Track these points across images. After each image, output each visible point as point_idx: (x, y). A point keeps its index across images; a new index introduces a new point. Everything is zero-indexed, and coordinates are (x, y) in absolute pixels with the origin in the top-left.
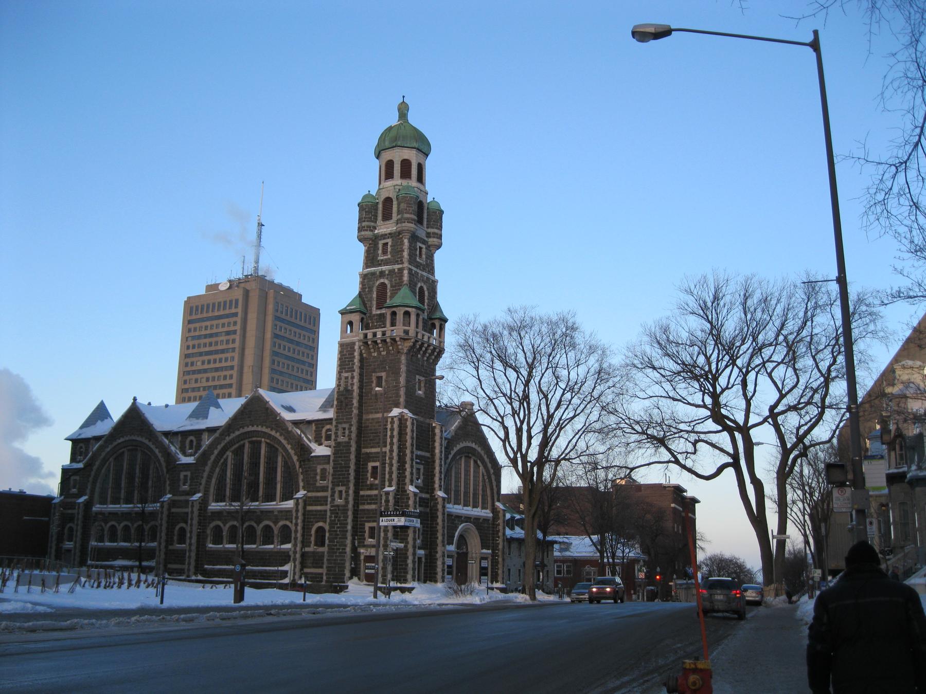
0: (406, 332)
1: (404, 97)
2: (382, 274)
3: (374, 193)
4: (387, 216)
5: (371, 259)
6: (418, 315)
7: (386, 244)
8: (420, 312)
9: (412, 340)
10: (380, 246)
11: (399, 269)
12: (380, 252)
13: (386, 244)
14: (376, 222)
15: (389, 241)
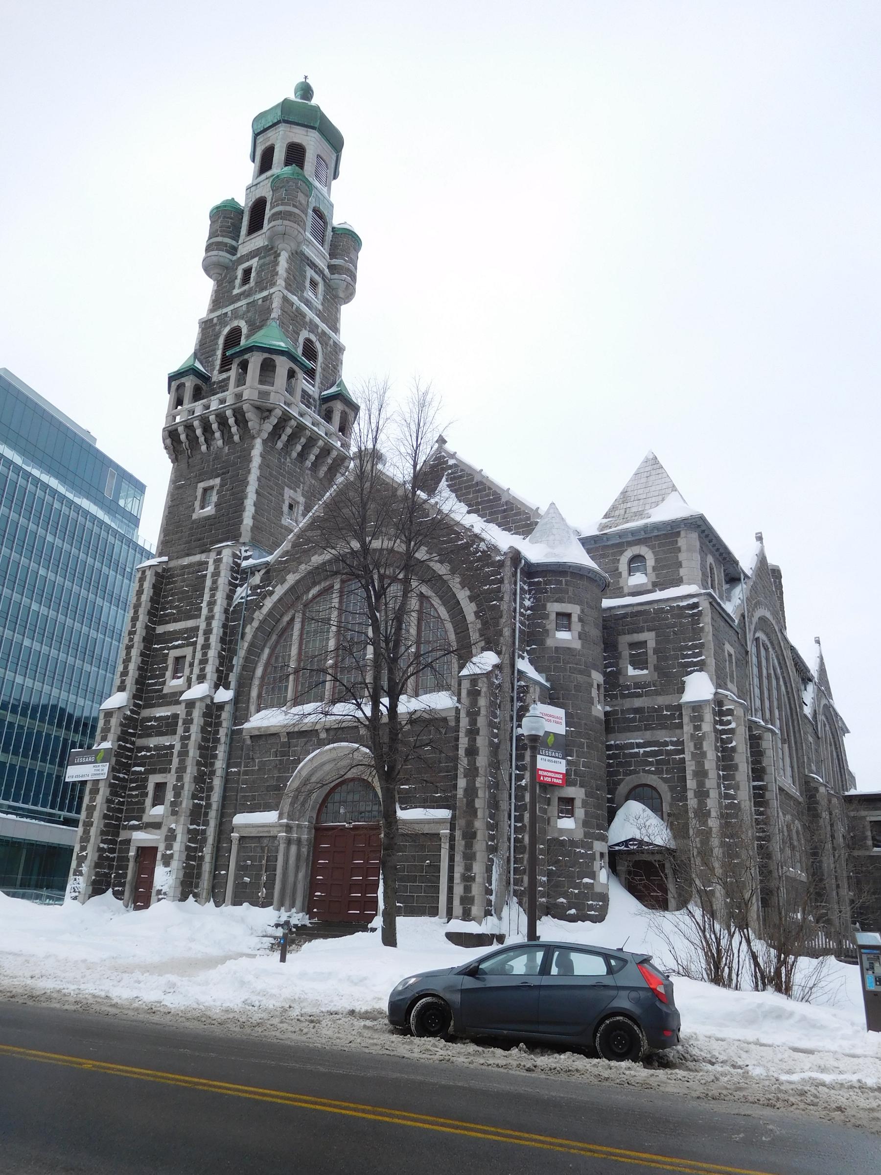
0: (264, 395)
1: (306, 77)
2: (236, 315)
3: (242, 200)
4: (256, 225)
5: (220, 299)
6: (291, 374)
7: (247, 272)
8: (297, 369)
9: (278, 413)
10: (240, 273)
11: (265, 299)
12: (238, 282)
13: (247, 272)
14: (236, 237)
15: (254, 262)
